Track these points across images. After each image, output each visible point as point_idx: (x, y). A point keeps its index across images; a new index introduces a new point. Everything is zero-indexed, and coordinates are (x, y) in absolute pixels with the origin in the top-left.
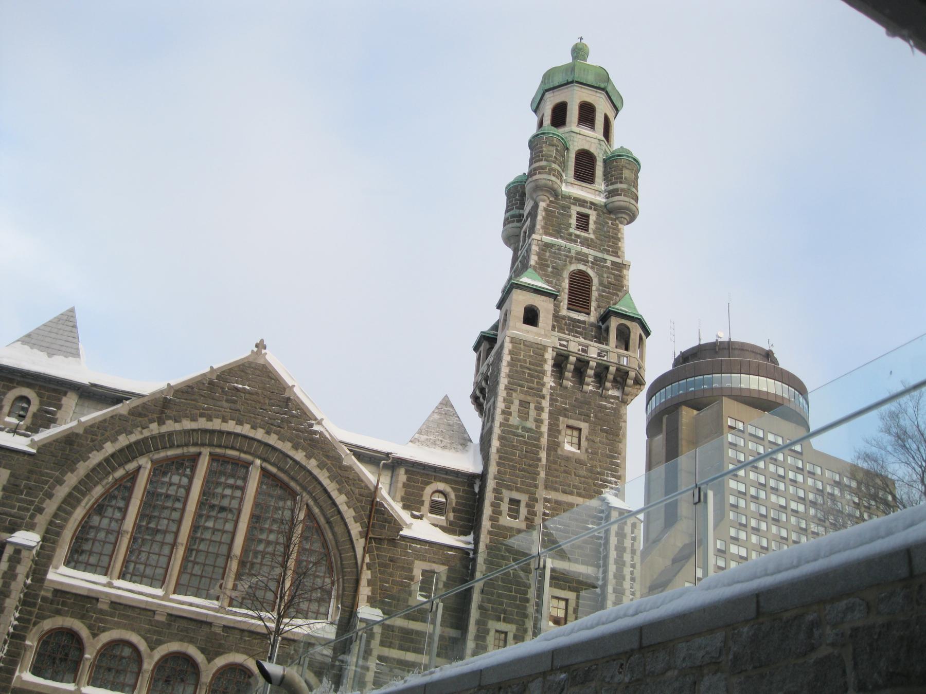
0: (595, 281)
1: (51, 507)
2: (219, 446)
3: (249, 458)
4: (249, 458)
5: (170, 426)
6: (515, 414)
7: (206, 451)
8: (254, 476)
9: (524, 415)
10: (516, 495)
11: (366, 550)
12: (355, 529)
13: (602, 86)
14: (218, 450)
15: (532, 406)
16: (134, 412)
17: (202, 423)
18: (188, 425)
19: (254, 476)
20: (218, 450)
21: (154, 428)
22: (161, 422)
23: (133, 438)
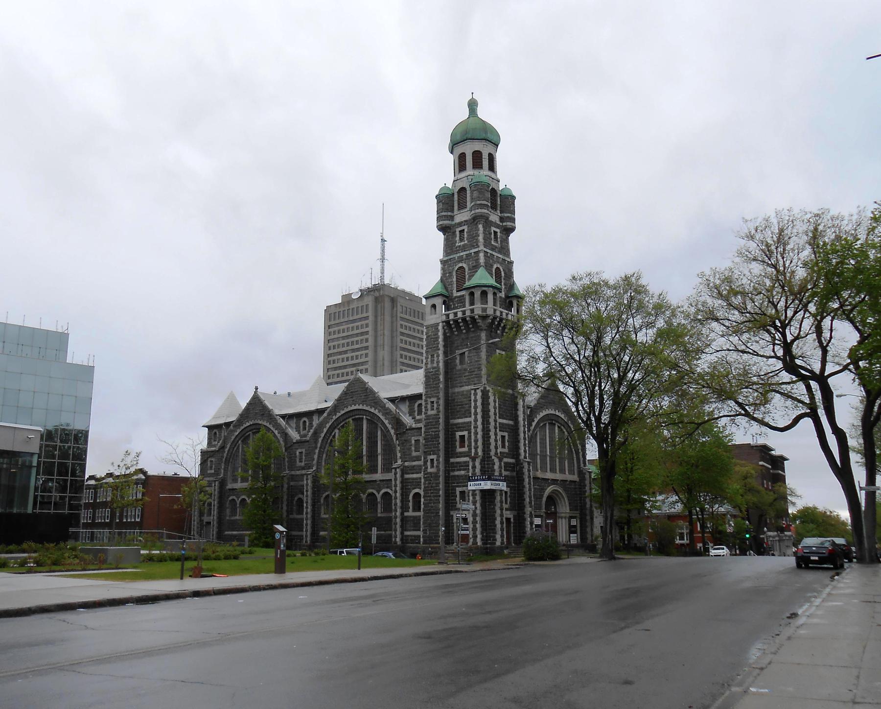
0: (467, 269)
1: (316, 457)
2: (353, 416)
3: (362, 416)
4: (362, 416)
5: (339, 415)
6: (429, 363)
7: (350, 419)
8: (365, 422)
9: (432, 361)
10: (432, 400)
11: (397, 440)
12: (392, 432)
13: (465, 138)
14: (353, 417)
15: (435, 355)
16: (329, 414)
17: (346, 410)
18: (342, 412)
19: (365, 422)
20: (353, 417)
21: (334, 418)
22: (336, 415)
23: (330, 424)
